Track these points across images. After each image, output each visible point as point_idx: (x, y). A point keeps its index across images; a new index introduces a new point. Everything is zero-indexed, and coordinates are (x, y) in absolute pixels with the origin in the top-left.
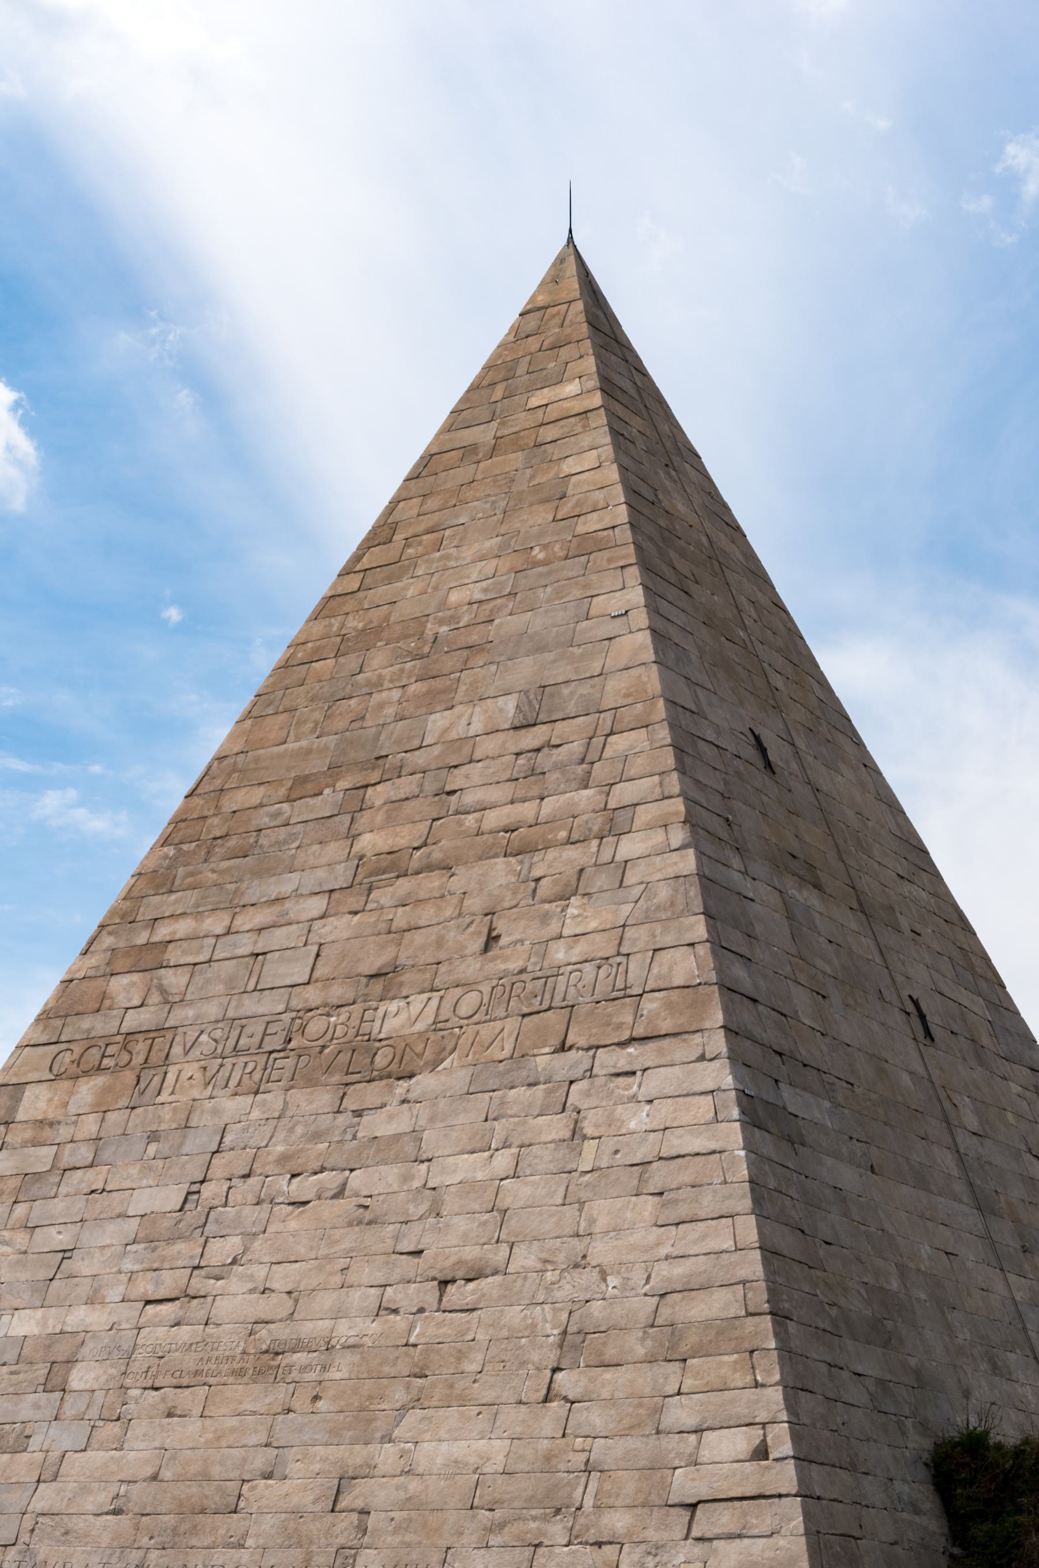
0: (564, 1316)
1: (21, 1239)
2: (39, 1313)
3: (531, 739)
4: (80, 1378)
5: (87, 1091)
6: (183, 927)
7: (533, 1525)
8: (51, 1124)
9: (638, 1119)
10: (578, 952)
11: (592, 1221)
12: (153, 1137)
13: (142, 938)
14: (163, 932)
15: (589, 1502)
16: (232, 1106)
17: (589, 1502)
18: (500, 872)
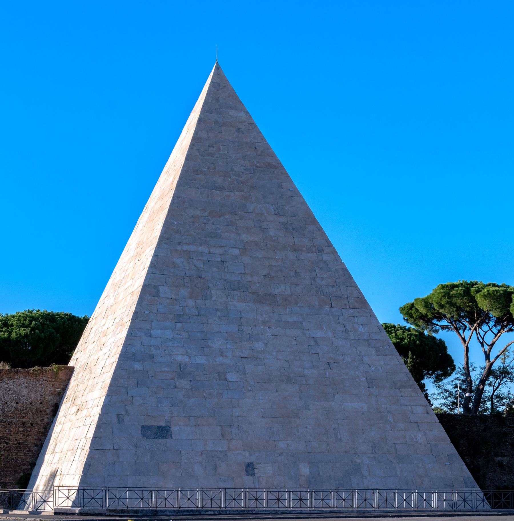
0: (365, 374)
1: (186, 335)
2: (205, 358)
3: (283, 219)
4: (231, 377)
5: (184, 292)
6: (192, 248)
7: (381, 425)
8: (176, 300)
9: (361, 329)
10: (324, 282)
11: (360, 352)
12: (218, 310)
13: (179, 248)
14: (186, 248)
15: (392, 421)
16: (240, 305)
17: (392, 421)
18: (291, 256)
